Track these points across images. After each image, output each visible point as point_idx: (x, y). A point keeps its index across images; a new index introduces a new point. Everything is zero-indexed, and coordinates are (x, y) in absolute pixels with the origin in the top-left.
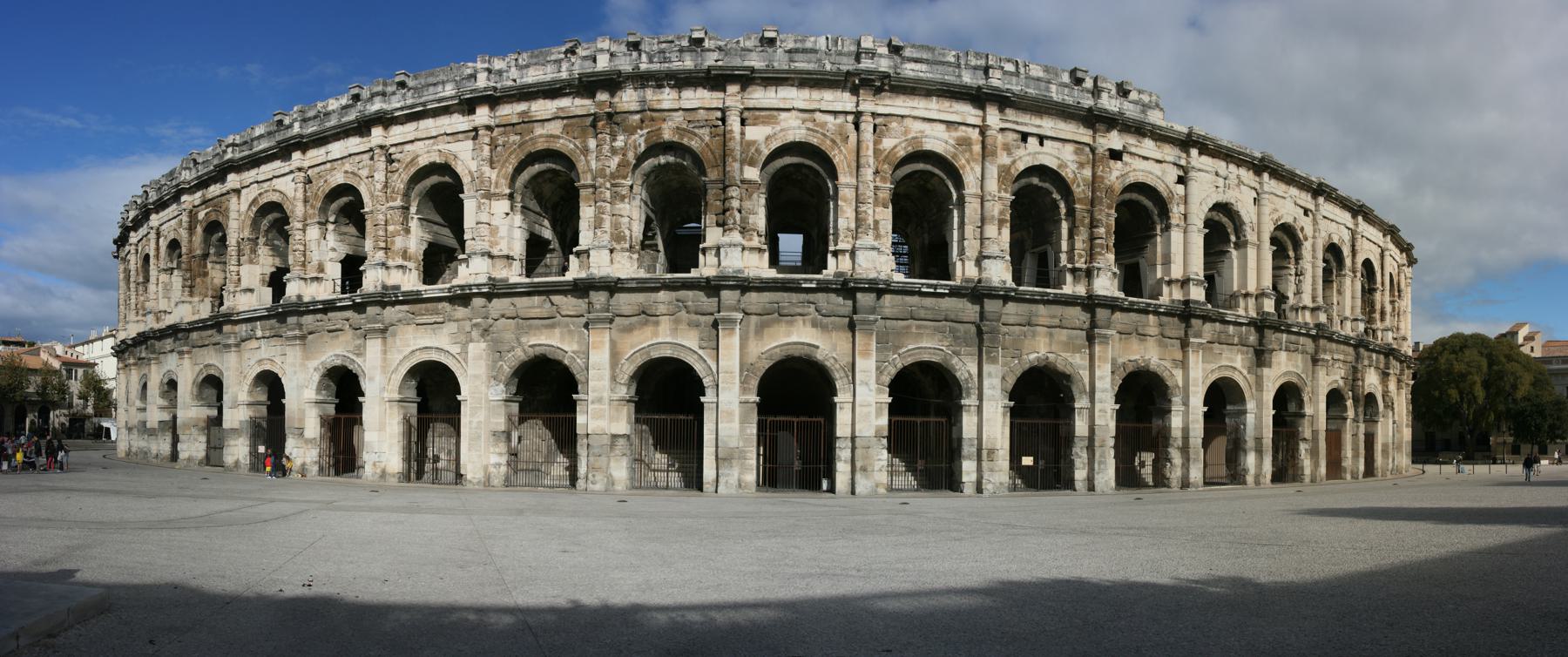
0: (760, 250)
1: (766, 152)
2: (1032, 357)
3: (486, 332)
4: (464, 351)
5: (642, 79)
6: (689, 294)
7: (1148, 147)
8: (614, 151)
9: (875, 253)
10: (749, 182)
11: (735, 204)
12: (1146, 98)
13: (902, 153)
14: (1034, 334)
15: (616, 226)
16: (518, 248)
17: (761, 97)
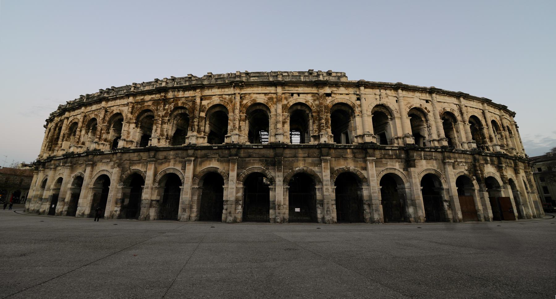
0: (204, 138)
1: (208, 108)
2: (297, 169)
5: (174, 89)
6: (180, 152)
9: (237, 136)
10: (202, 117)
13: (250, 104)
14: (298, 161)
17: (207, 92)
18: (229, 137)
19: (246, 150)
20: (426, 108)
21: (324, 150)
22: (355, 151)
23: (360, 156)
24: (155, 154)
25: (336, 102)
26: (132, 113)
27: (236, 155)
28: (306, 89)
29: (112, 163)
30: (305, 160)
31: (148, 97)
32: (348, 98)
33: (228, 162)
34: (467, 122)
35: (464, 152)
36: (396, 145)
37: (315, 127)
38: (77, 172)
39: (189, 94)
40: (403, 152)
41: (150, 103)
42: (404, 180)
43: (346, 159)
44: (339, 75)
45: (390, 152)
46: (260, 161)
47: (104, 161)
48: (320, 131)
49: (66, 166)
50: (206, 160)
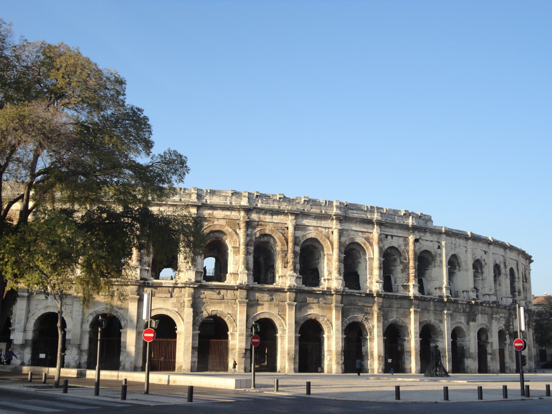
1: (302, 241)
2: (391, 320)
13: (348, 243)
20: (484, 260)
22: (436, 304)
25: (423, 249)
28: (399, 231)
29: (174, 300)
30: (397, 311)
32: (432, 246)
34: (509, 276)
35: (505, 307)
39: (277, 219)
40: (468, 306)
41: (223, 222)
42: (466, 334)
44: (426, 218)
45: (460, 306)
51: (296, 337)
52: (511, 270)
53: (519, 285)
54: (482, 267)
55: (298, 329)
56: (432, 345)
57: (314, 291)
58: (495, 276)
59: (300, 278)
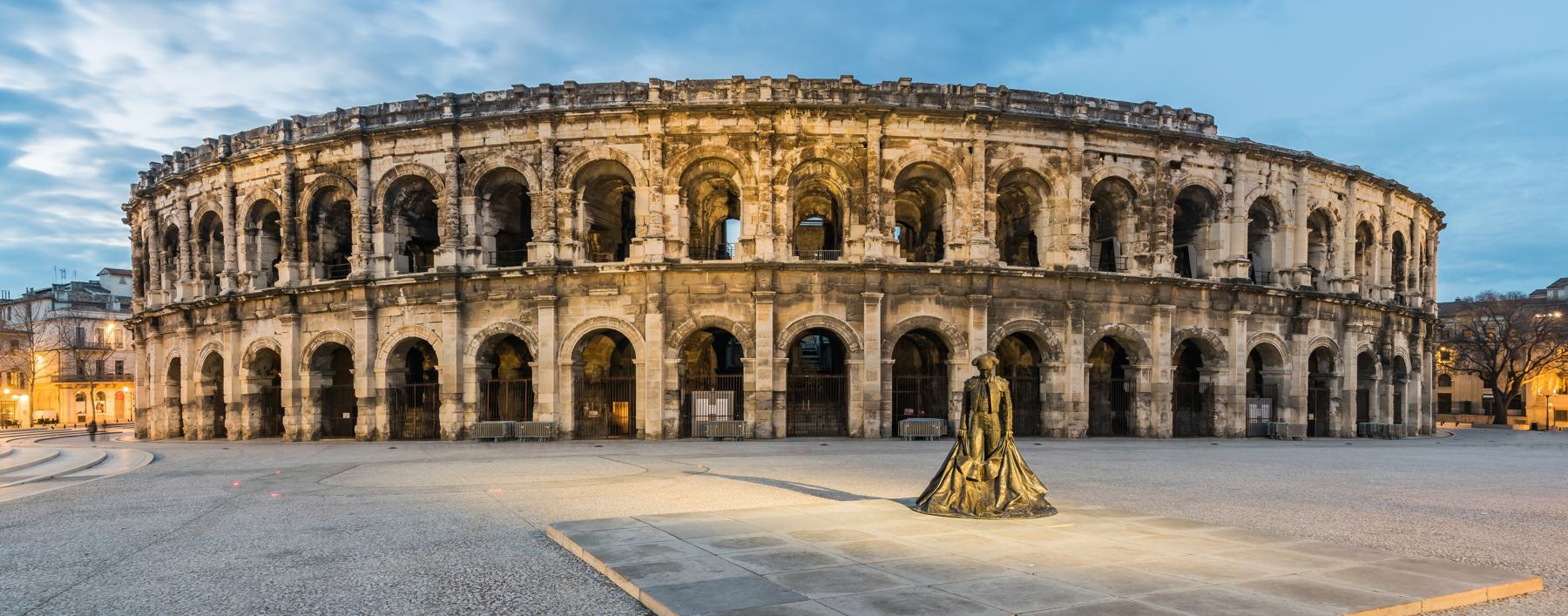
0: (895, 244)
3: (663, 306)
4: (640, 324)
6: (840, 276)
7: (1203, 157)
8: (774, 163)
9: (987, 247)
11: (877, 207)
12: (1202, 119)
14: (1108, 309)
15: (775, 220)
16: (685, 238)
18: (960, 246)
19: (1003, 281)
21: (1164, 292)
23: (1222, 306)
24: (773, 280)
26: (663, 164)
27: (987, 291)
29: (626, 300)
30: (1121, 310)
31: (709, 124)
33: (964, 305)
34: (1390, 247)
35: (1377, 306)
36: (1279, 286)
37: (1144, 236)
38: (495, 319)
43: (1196, 310)
46: (1032, 306)
47: (593, 292)
48: (1153, 246)
49: (442, 307)
50: (909, 299)
51: (883, 365)
52: (1398, 235)
53: (1411, 266)
54: (1329, 225)
55: (891, 348)
56: (1204, 379)
57: (926, 269)
58: (1358, 246)
59: (895, 244)
